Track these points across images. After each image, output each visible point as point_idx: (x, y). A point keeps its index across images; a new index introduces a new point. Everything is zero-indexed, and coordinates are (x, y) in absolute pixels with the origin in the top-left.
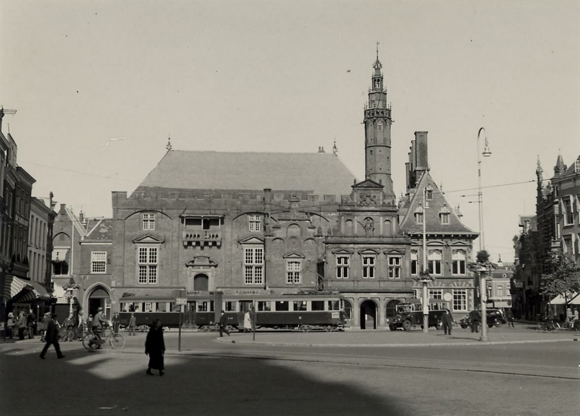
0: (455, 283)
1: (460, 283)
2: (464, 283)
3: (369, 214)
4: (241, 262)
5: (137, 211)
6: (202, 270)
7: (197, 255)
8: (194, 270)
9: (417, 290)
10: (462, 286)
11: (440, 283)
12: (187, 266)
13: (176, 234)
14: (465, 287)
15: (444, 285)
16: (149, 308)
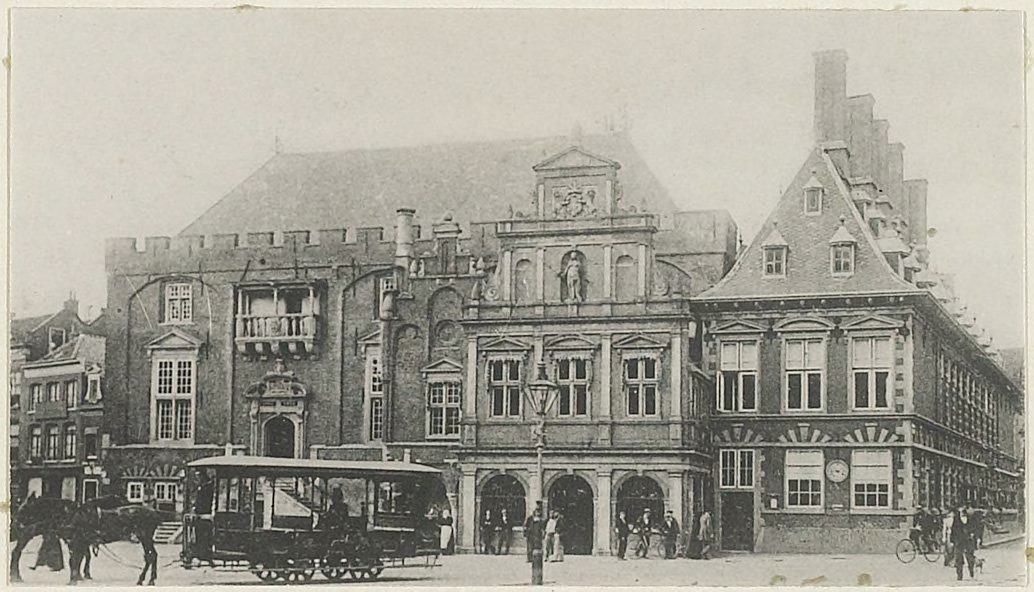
0: (858, 433)
1: (871, 432)
2: (884, 432)
3: (573, 241)
4: (363, 389)
5: (152, 278)
6: (279, 409)
7: (269, 373)
8: (264, 409)
9: (753, 450)
10: (876, 440)
11: (817, 433)
12: (250, 400)
13: (229, 329)
14: (884, 444)
15: (827, 438)
16: (174, 495)
